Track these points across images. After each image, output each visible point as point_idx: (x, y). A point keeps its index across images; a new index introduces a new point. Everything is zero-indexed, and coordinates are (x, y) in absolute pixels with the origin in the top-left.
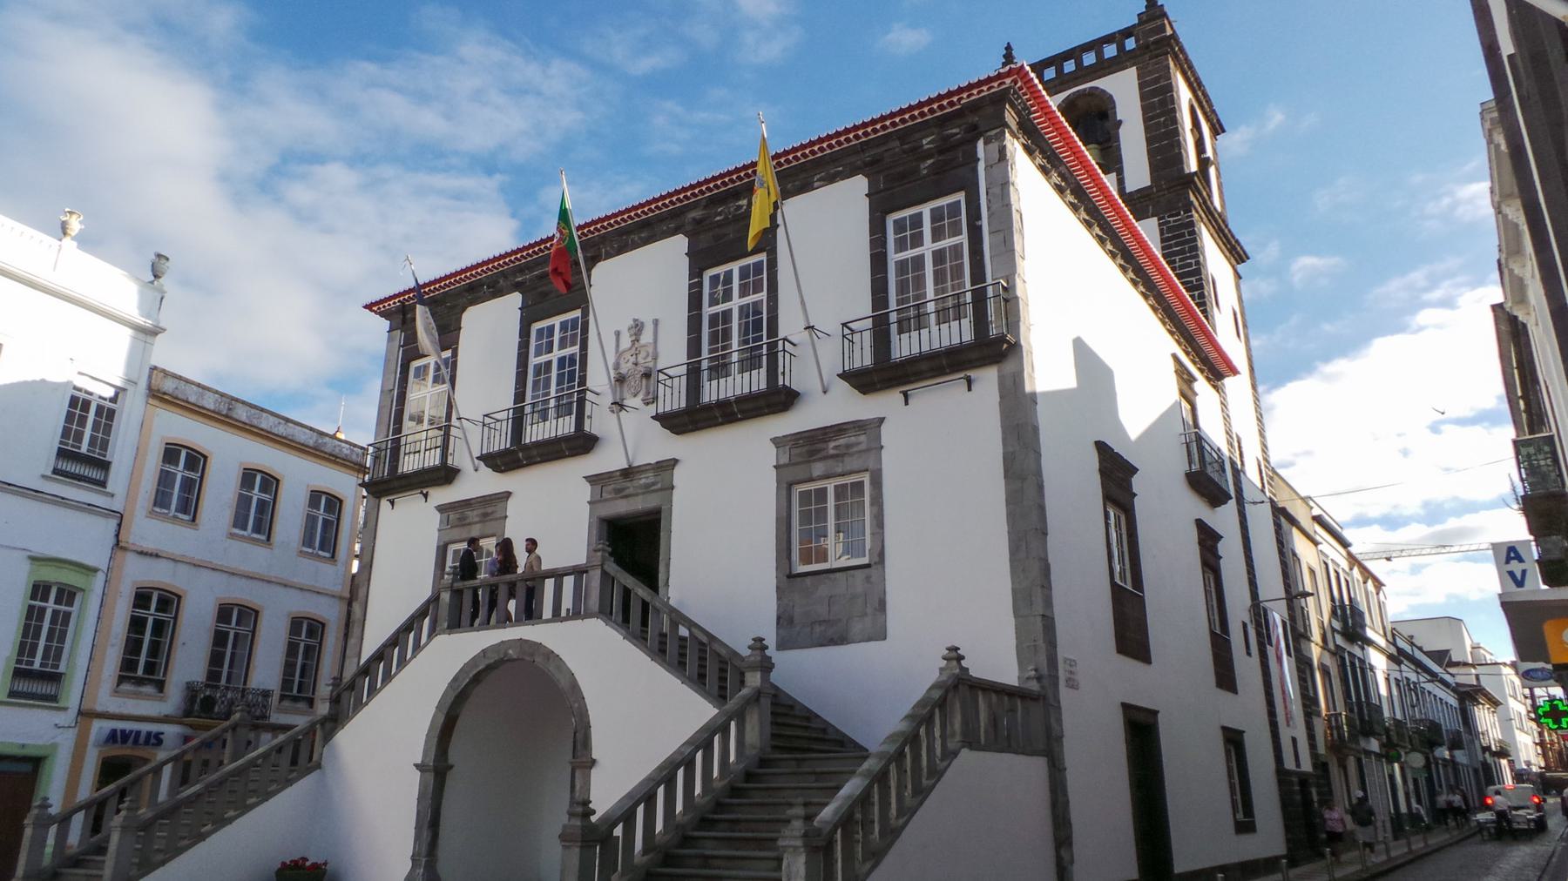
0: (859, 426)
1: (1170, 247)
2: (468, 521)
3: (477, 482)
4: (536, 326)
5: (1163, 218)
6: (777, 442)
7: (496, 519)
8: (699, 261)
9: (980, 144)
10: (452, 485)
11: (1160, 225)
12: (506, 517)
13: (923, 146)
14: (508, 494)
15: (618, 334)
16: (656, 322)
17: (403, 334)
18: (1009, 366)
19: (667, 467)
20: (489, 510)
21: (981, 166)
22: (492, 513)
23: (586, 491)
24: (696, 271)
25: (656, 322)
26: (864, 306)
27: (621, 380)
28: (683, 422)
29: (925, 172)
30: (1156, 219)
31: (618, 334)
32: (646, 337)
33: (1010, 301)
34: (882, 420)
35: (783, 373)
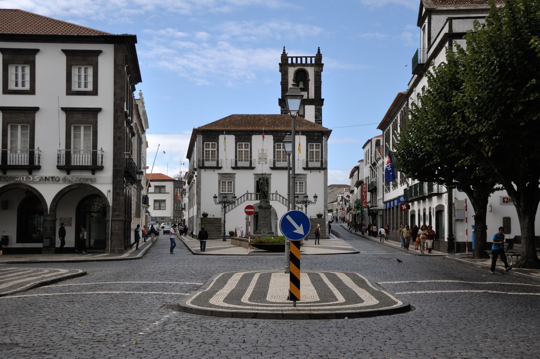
0: (304, 175)
3: (227, 169)
4: (238, 143)
9: (324, 137)
14: (235, 174)
15: (259, 150)
16: (267, 150)
18: (325, 171)
19: (270, 174)
21: (324, 141)
23: (253, 176)
24: (274, 143)
25: (267, 150)
26: (305, 158)
27: (260, 158)
28: (274, 168)
31: (259, 150)
32: (265, 152)
33: (326, 162)
34: (307, 174)
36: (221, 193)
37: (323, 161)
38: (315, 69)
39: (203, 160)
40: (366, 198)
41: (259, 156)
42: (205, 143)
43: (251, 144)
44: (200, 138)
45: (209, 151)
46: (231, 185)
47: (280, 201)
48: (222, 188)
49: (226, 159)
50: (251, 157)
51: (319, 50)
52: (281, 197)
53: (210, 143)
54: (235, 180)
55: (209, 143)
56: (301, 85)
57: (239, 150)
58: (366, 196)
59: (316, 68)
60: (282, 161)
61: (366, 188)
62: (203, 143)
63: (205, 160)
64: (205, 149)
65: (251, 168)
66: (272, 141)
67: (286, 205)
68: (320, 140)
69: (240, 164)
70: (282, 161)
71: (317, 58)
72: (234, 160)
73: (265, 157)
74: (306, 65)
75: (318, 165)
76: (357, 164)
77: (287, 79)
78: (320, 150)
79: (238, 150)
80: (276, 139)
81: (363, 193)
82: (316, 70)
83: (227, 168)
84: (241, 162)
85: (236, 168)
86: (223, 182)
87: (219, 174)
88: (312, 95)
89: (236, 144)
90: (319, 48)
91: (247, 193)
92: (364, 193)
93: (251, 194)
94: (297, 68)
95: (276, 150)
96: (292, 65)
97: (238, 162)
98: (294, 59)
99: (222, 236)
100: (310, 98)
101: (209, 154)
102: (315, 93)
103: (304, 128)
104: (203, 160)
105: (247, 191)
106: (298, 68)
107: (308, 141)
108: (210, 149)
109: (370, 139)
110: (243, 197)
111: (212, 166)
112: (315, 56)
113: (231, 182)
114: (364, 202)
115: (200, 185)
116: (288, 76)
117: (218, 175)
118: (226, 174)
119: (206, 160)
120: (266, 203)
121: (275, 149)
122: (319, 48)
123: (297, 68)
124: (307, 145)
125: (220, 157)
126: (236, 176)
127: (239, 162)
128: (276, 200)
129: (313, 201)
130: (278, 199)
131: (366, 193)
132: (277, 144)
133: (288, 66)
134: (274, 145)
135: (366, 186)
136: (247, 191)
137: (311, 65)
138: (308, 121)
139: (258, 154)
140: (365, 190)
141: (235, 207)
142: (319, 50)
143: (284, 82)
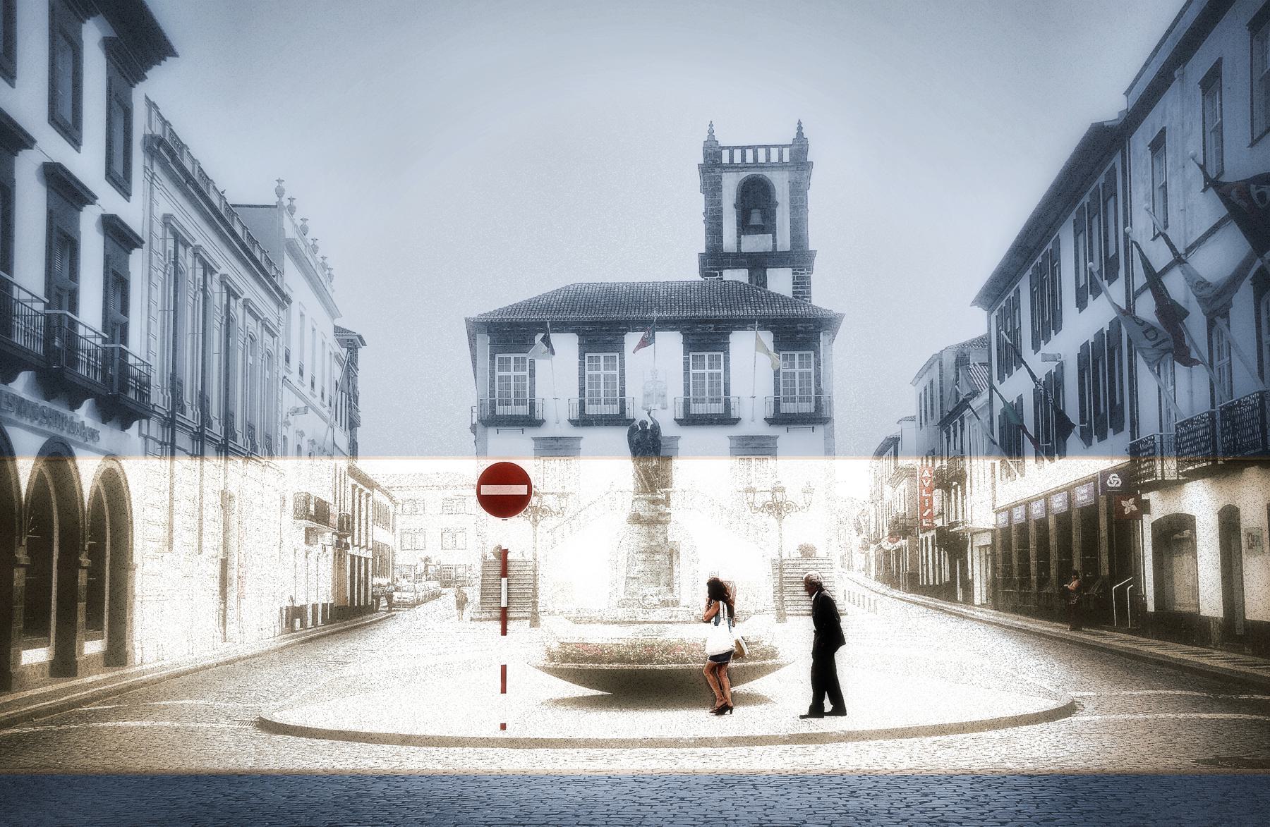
1: (797, 288)
4: (587, 355)
5: (795, 270)
6: (731, 438)
9: (821, 334)
11: (793, 274)
14: (579, 439)
18: (828, 426)
19: (677, 438)
21: (821, 343)
24: (686, 352)
27: (647, 396)
30: (791, 269)
40: (931, 506)
41: (644, 388)
42: (497, 356)
44: (484, 342)
51: (800, 128)
53: (512, 356)
55: (508, 355)
56: (756, 218)
57: (590, 372)
58: (931, 499)
60: (707, 400)
63: (497, 402)
64: (498, 374)
70: (707, 400)
71: (795, 148)
74: (769, 165)
76: (893, 431)
78: (812, 370)
79: (587, 373)
87: (535, 439)
88: (784, 242)
90: (800, 123)
95: (692, 371)
96: (732, 166)
97: (586, 405)
98: (737, 154)
100: (778, 250)
102: (793, 238)
103: (766, 312)
106: (748, 174)
114: (925, 515)
117: (533, 442)
118: (557, 439)
120: (652, 506)
122: (800, 123)
123: (744, 175)
127: (591, 406)
129: (801, 503)
137: (781, 165)
138: (777, 295)
142: (800, 128)
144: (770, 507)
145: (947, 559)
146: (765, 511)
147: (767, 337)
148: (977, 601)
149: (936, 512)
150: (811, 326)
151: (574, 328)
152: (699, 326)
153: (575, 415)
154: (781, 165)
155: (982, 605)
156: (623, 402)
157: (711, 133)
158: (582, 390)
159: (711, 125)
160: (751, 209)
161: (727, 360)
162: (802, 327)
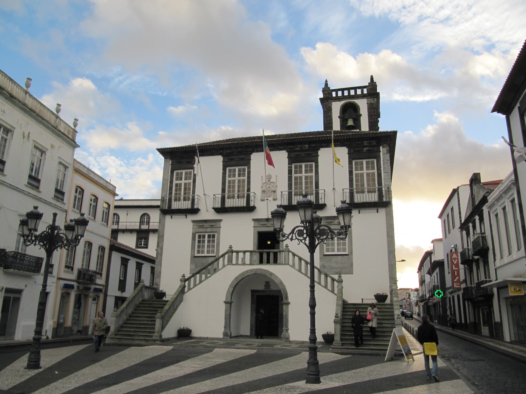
2: (205, 227)
7: (217, 227)
8: (292, 160)
9: (381, 147)
10: (197, 214)
12: (220, 227)
13: (364, 144)
14: (220, 221)
15: (262, 177)
16: (276, 176)
17: (171, 161)
20: (214, 224)
21: (381, 153)
22: (215, 225)
23: (252, 223)
24: (290, 163)
25: (276, 176)
26: (347, 186)
27: (264, 192)
29: (365, 151)
33: (389, 191)
35: (321, 199)
36: (196, 255)
37: (383, 189)
38: (367, 101)
39: (170, 200)
40: (458, 275)
41: (262, 187)
43: (249, 168)
45: (181, 184)
46: (213, 241)
47: (293, 266)
48: (199, 247)
49: (205, 195)
50: (249, 190)
52: (296, 258)
54: (220, 233)
56: (350, 123)
57: (230, 179)
58: (458, 271)
59: (369, 99)
61: (458, 259)
62: (172, 172)
64: (175, 182)
65: (249, 209)
66: (287, 160)
67: (306, 275)
68: (374, 154)
69: (229, 203)
72: (220, 196)
73: (273, 189)
74: (356, 96)
75: (374, 198)
77: (331, 117)
78: (375, 171)
79: (227, 179)
80: (292, 156)
81: (454, 266)
82: (369, 102)
83: (207, 211)
84: (232, 200)
85: (222, 210)
86: (199, 237)
87: (193, 222)
89: (224, 170)
91: (231, 251)
92: (455, 267)
93: (245, 252)
94: (343, 102)
95: (294, 175)
96: (337, 99)
99: (154, 338)
101: (180, 190)
104: (170, 200)
105: (231, 247)
107: (351, 157)
108: (183, 182)
109: (456, 188)
110: (221, 259)
111: (182, 208)
112: (368, 85)
113: (214, 236)
114: (455, 280)
115: (163, 241)
116: (331, 113)
117: (192, 224)
118: (206, 221)
119: (176, 200)
121: (292, 174)
123: (343, 102)
124: (350, 163)
125: (197, 193)
126: (222, 224)
128: (285, 264)
130: (291, 263)
131: (457, 266)
132: (295, 166)
133: (331, 101)
134: (289, 167)
135: (457, 255)
136: (231, 247)
139: (261, 185)
140: (455, 262)
141: (206, 278)
143: (327, 120)
144: (300, 233)
145: (470, 308)
146: (294, 238)
147: (343, 152)
148: (507, 338)
149: (461, 280)
150: (373, 143)
151: (221, 151)
152: (299, 146)
153: (219, 205)
154: (363, 96)
155: (511, 342)
156: (248, 196)
157: (326, 84)
158: (223, 190)
159: (326, 81)
160: (348, 119)
161: (317, 166)
162: (366, 143)
